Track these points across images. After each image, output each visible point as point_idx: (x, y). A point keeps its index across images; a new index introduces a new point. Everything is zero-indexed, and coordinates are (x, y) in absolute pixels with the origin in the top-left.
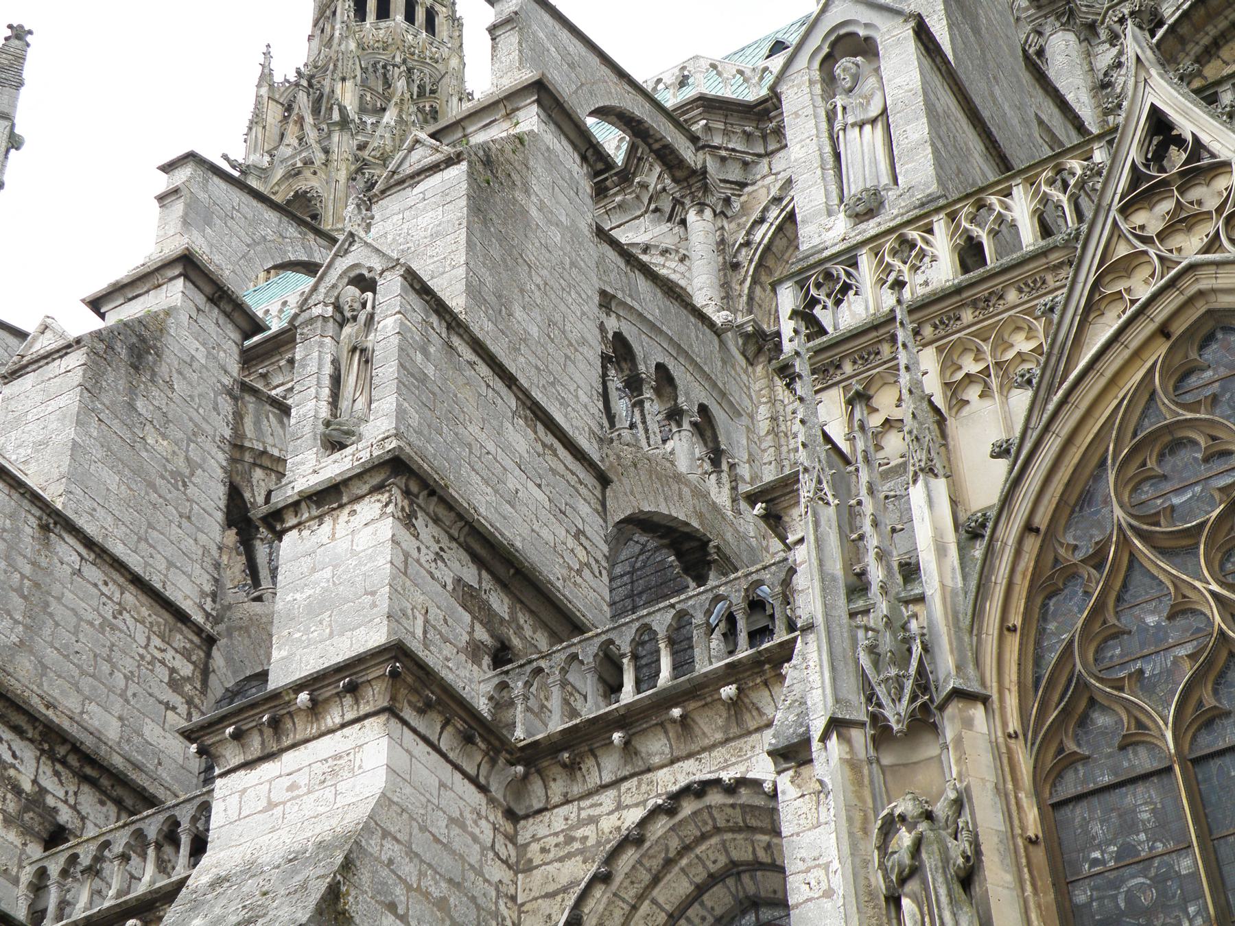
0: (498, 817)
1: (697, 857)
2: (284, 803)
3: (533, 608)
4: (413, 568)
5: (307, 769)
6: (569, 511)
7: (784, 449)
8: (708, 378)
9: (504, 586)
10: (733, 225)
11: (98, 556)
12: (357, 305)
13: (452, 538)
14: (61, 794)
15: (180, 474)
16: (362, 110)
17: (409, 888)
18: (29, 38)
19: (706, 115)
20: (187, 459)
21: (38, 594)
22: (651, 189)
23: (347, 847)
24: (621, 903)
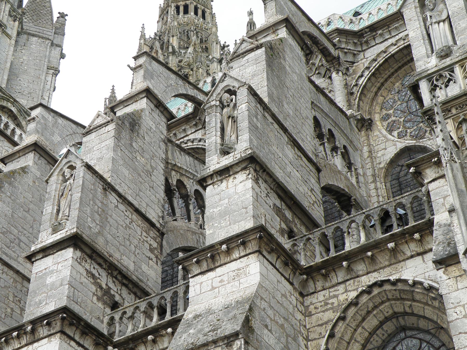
0: (297, 295)
1: (380, 310)
2: (219, 287)
3: (300, 217)
4: (260, 199)
6: (308, 181)
7: (375, 163)
8: (346, 135)
9: (290, 208)
10: (350, 78)
11: (123, 201)
12: (229, 101)
13: (271, 189)
14: (116, 290)
15: (149, 171)
16: (180, 48)
17: (271, 319)
18: (66, 18)
19: (339, 36)
20: (151, 166)
21: (104, 214)
22: (316, 65)
23: (249, 302)
24: (350, 328)
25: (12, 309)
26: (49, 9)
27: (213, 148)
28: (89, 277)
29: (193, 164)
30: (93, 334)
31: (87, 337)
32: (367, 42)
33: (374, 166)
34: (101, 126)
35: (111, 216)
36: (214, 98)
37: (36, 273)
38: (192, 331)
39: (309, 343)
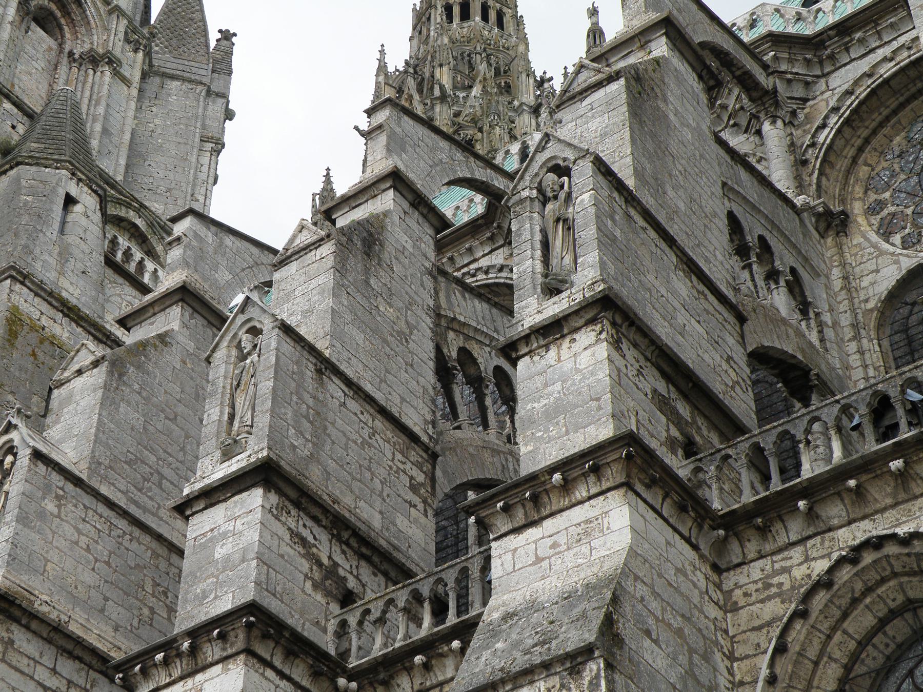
1: (879, 596)
2: (549, 558)
3: (707, 413)
4: (624, 380)
5: (564, 532)
6: (720, 342)
7: (856, 301)
8: (794, 246)
9: (685, 396)
10: (799, 132)
11: (355, 392)
12: (556, 187)
13: (647, 359)
14: (348, 567)
15: (403, 333)
16: (455, 88)
17: (657, 619)
18: (234, 39)
19: (774, 48)
20: (407, 322)
21: (319, 420)
22: (730, 109)
23: (612, 586)
24: (818, 633)
25: (152, 609)
26: (201, 24)
27: (528, 282)
28: (295, 543)
29: (488, 317)
30: (307, 654)
31: (297, 661)
32: (832, 57)
33: (856, 307)
34: (307, 248)
35: (333, 424)
36: (527, 183)
37: (195, 539)
38: (499, 645)
39: (735, 665)
